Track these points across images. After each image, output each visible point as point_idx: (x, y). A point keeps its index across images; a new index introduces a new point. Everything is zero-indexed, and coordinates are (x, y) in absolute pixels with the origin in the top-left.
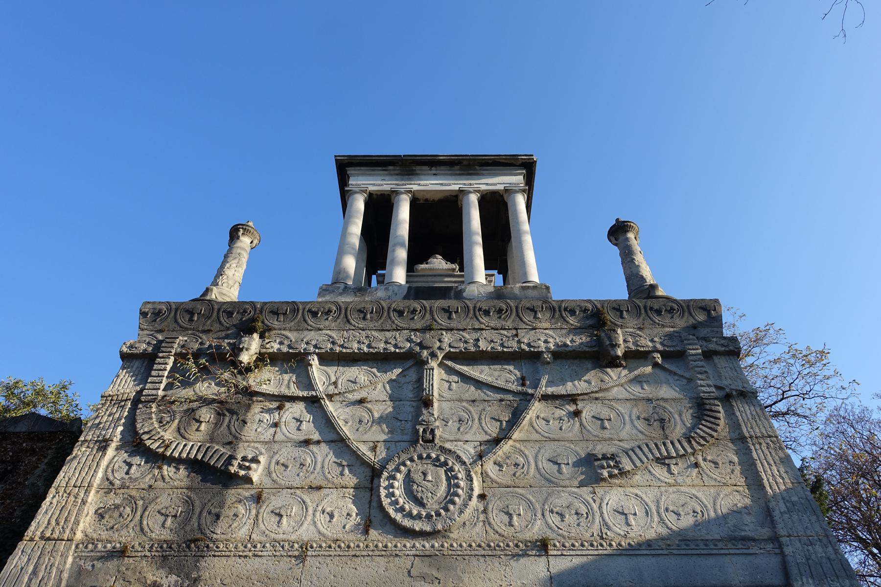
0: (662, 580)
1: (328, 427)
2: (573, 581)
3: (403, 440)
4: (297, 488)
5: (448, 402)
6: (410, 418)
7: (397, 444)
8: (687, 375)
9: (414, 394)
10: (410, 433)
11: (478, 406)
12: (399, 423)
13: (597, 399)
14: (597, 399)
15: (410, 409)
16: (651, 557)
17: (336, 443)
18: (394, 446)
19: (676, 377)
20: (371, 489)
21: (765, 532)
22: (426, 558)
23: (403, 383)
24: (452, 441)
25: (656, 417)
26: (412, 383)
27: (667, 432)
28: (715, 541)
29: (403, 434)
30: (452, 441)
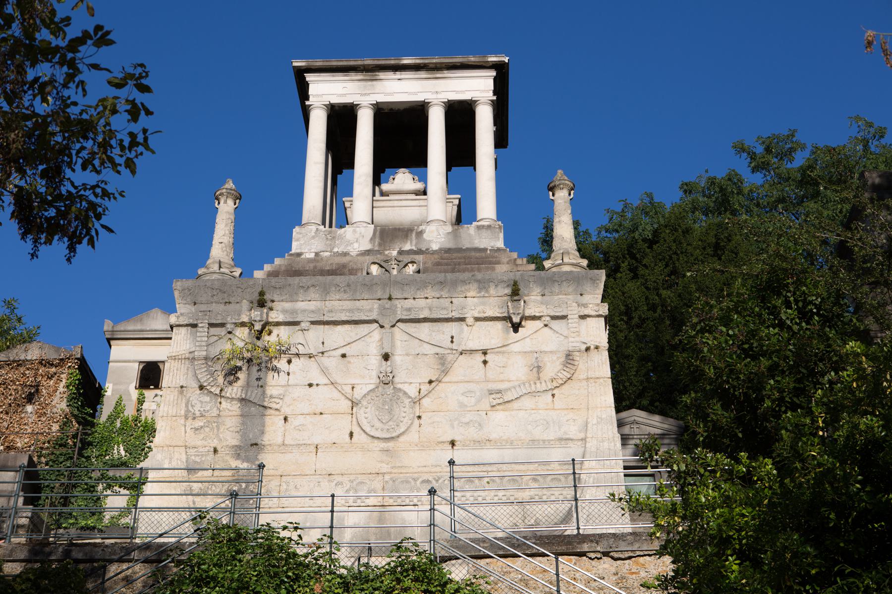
8: (565, 333)
12: (368, 371)
13: (500, 352)
14: (500, 352)
15: (375, 362)
19: (557, 335)
20: (352, 414)
21: (582, 435)
25: (536, 365)
27: (541, 375)
28: (549, 441)
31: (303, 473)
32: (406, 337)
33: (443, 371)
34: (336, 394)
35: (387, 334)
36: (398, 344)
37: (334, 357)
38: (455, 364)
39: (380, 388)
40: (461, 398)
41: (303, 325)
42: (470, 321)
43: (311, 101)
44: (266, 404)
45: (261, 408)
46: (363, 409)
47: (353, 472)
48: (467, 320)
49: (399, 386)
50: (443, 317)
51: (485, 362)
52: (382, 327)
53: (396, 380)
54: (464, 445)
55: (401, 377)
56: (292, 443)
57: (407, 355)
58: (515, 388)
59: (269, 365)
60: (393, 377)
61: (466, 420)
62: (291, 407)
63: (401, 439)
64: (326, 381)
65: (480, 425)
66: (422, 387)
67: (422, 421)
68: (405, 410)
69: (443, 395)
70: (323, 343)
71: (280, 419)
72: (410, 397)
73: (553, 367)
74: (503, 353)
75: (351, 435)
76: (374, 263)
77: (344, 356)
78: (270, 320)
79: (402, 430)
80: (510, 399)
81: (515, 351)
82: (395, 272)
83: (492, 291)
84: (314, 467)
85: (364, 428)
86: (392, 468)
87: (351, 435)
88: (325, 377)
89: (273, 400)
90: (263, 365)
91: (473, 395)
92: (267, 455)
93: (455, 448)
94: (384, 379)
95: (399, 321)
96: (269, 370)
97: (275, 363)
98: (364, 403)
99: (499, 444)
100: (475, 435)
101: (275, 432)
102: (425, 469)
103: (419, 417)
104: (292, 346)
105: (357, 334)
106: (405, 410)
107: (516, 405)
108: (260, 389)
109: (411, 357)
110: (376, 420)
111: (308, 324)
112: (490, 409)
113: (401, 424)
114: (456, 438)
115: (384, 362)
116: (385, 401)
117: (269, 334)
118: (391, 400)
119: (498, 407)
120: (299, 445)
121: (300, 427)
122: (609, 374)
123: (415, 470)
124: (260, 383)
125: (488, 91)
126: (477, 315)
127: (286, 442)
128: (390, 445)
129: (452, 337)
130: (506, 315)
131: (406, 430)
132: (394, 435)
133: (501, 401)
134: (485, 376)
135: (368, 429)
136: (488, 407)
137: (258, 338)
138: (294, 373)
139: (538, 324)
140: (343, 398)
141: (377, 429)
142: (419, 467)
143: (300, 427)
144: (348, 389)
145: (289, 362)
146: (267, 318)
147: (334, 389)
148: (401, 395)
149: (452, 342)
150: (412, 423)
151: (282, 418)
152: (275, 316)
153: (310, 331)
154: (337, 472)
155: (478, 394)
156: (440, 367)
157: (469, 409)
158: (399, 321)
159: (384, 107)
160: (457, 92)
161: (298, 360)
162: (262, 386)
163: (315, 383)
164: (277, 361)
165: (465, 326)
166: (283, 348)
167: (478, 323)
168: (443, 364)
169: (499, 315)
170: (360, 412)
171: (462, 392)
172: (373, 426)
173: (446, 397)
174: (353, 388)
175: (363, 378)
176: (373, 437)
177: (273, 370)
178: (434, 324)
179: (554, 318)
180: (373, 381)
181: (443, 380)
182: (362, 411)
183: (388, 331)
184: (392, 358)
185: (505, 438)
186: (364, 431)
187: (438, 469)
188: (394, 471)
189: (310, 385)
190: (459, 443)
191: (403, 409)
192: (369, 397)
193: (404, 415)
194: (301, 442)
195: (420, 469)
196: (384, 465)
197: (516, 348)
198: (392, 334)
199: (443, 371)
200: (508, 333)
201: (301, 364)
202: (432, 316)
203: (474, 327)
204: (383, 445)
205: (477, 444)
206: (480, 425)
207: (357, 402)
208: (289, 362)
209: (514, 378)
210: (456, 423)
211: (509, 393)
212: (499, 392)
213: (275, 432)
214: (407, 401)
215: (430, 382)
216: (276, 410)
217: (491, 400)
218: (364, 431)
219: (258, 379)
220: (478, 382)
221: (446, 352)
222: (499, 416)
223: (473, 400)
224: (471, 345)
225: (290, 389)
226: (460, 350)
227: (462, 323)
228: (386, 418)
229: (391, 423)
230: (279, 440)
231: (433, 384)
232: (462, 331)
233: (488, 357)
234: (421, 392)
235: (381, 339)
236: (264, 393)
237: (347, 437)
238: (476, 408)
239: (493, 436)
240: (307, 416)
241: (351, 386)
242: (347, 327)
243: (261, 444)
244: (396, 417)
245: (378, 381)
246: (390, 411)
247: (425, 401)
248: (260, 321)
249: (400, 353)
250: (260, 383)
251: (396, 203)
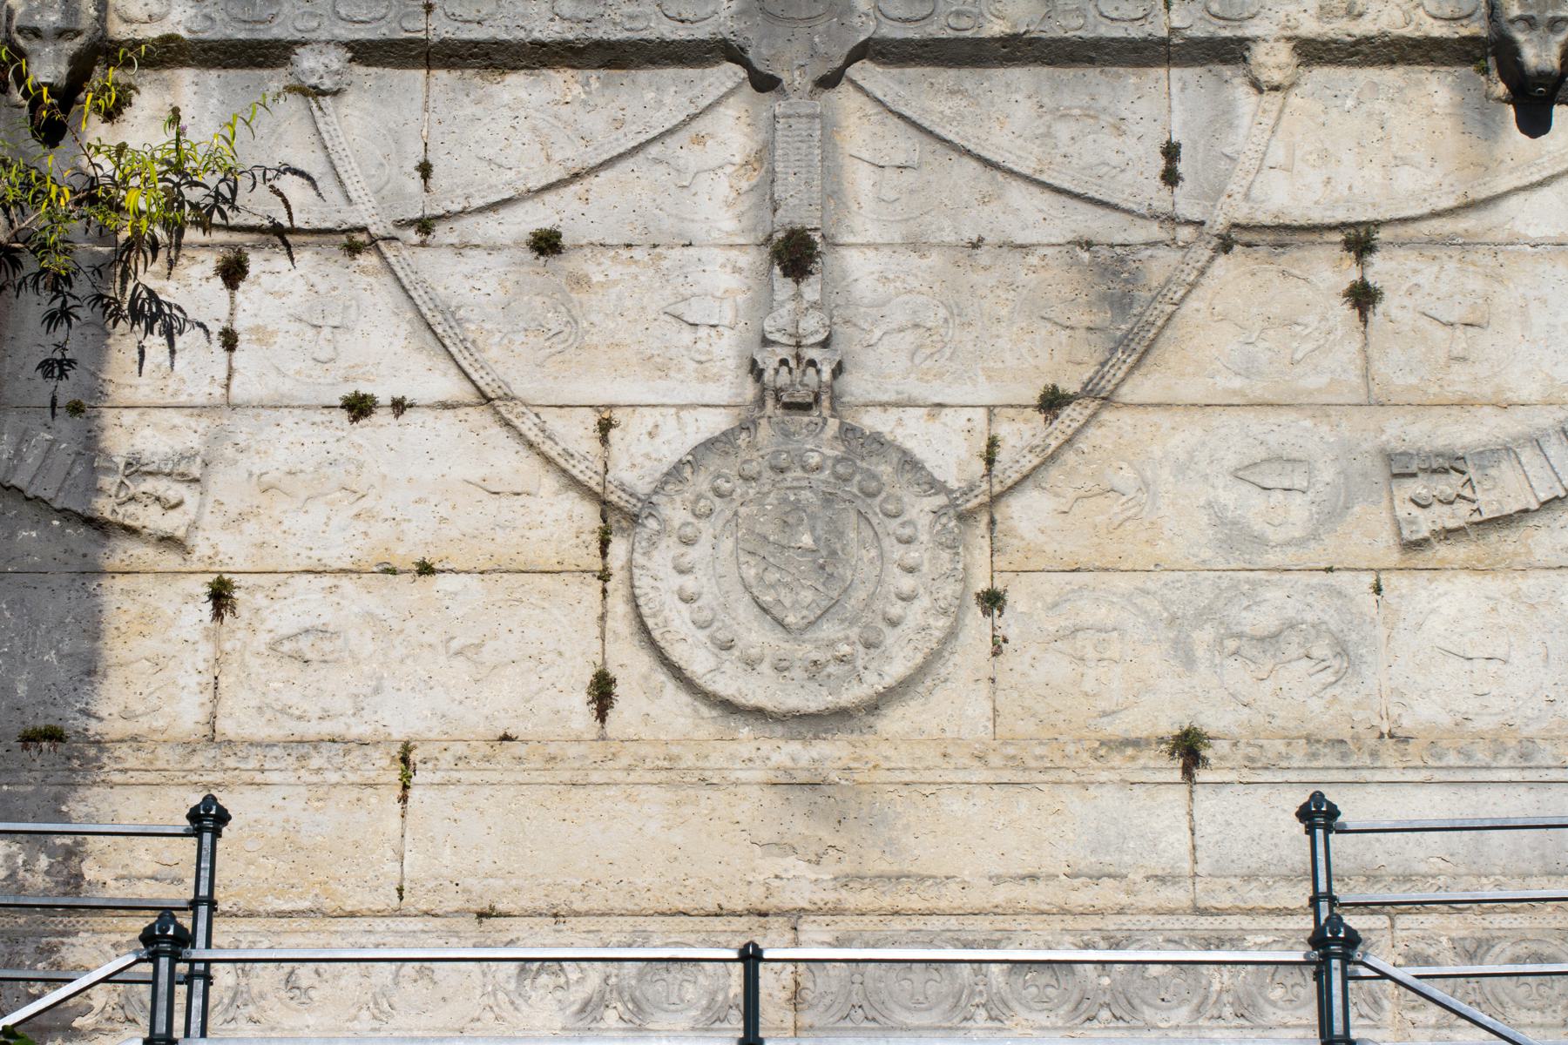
0: (1543, 856)
1: (420, 350)
2: (1264, 857)
3: (706, 400)
4: (342, 571)
5: (871, 253)
6: (728, 316)
7: (683, 414)
9: (739, 217)
10: (730, 377)
11: (985, 269)
12: (687, 336)
13: (1447, 242)
14: (1447, 242)
16: (1522, 789)
17: (461, 412)
18: (671, 422)
22: (797, 791)
23: (693, 169)
24: (884, 405)
26: (729, 169)
29: (704, 378)
30: (884, 405)
31: (329, 905)
32: (904, 145)
33: (1124, 343)
34: (509, 462)
35: (801, 126)
36: (861, 181)
37: (493, 249)
38: (1192, 303)
39: (764, 432)
40: (1230, 496)
41: (310, 64)
42: (1273, 60)
44: (104, 507)
45: (76, 533)
47: (617, 902)
48: (1259, 54)
49: (872, 421)
50: (1117, 32)
51: (1363, 297)
52: (764, 83)
53: (856, 385)
54: (1251, 763)
56: (262, 731)
57: (915, 245)
58: (1537, 443)
59: (114, 291)
60: (838, 370)
61: (1262, 620)
62: (250, 527)
63: (894, 721)
65: (1342, 649)
66: (1004, 430)
67: (1009, 624)
68: (913, 555)
69: (1125, 478)
70: (425, 170)
71: (190, 598)
72: (935, 486)
74: (1466, 244)
75: (602, 691)
77: (546, 244)
78: (119, 30)
79: (897, 669)
80: (1512, 507)
81: (1534, 233)
84: (392, 868)
85: (677, 653)
86: (845, 881)
87: (602, 691)
88: (443, 364)
89: (149, 485)
90: (82, 287)
91: (1299, 481)
92: (117, 795)
93: (1202, 775)
94: (784, 378)
95: (863, 51)
96: (117, 316)
97: (149, 276)
98: (675, 512)
99: (1452, 759)
100: (1316, 705)
101: (158, 667)
102: (1034, 895)
103: (992, 601)
104: (244, 182)
105: (619, 123)
106: (913, 555)
108: (66, 425)
109: (935, 259)
110: (744, 609)
111: (336, 59)
112: (1394, 558)
113: (890, 636)
114: (1209, 721)
115: (784, 287)
116: (797, 506)
117: (111, 115)
118: (828, 499)
119: (1443, 551)
120: (301, 747)
121: (304, 644)
123: (975, 900)
124: (66, 391)
126: (1310, 27)
127: (226, 727)
128: (830, 752)
129: (1171, 152)
130: (1477, 28)
131: (922, 671)
132: (851, 695)
133: (1460, 515)
134: (1366, 375)
135: (698, 661)
136: (1385, 550)
137: (52, 133)
138: (262, 335)
140: (550, 482)
141: (751, 664)
142: (997, 880)
143: (304, 644)
144: (576, 434)
145: (233, 272)
146: (102, 19)
147: (497, 433)
148: (885, 470)
149: (1171, 177)
150: (952, 634)
151: (200, 587)
153: (350, 98)
154: (525, 902)
155: (1327, 474)
156: (1102, 317)
157: (1274, 558)
158: (863, 51)
161: (281, 261)
162: (76, 409)
163: (384, 396)
164: (160, 265)
165: (1241, 93)
166: (193, 195)
167: (1320, 74)
168: (1121, 303)
169: (1438, 30)
171: (1232, 461)
172: (727, 646)
173: (1145, 486)
174: (605, 427)
175: (663, 370)
176: (729, 707)
177: (136, 314)
178: (1067, 74)
180: (720, 392)
181: (1127, 393)
182: (662, 558)
183: (805, 107)
184: (828, 261)
185: (1484, 723)
186: (677, 672)
187: (1108, 895)
188: (851, 899)
189: (359, 407)
190: (1222, 747)
191: (898, 552)
192: (702, 482)
193: (907, 583)
194: (312, 729)
195: (1001, 895)
196: (793, 865)
198: (829, 129)
199: (1124, 343)
200: (1489, 130)
201: (300, 288)
202: (1053, 31)
203: (1294, 100)
205: (1329, 758)
206: (1342, 649)
207: (632, 506)
208: (233, 272)
209: (1529, 390)
210: (1203, 637)
211: (1506, 472)
212: (1449, 464)
213: (158, 667)
214: (921, 508)
215: (1052, 402)
216: (168, 541)
217: (1404, 510)
218: (677, 672)
219: (56, 367)
220: (1322, 409)
221: (1141, 232)
223: (1299, 512)
225: (242, 427)
226: (1219, 222)
227: (1227, 71)
228: (800, 601)
229: (829, 630)
230: (188, 715)
231: (1071, 415)
232: (1224, 118)
233: (1380, 269)
234: (1003, 456)
235: (763, 157)
236: (90, 446)
237: (579, 704)
238: (1316, 555)
239: (1422, 713)
240: (345, 582)
241: (592, 419)
242: (561, 82)
243: (83, 735)
244: (861, 594)
245: (750, 390)
246: (826, 562)
248: (61, 34)
249: (872, 233)
250: (66, 391)
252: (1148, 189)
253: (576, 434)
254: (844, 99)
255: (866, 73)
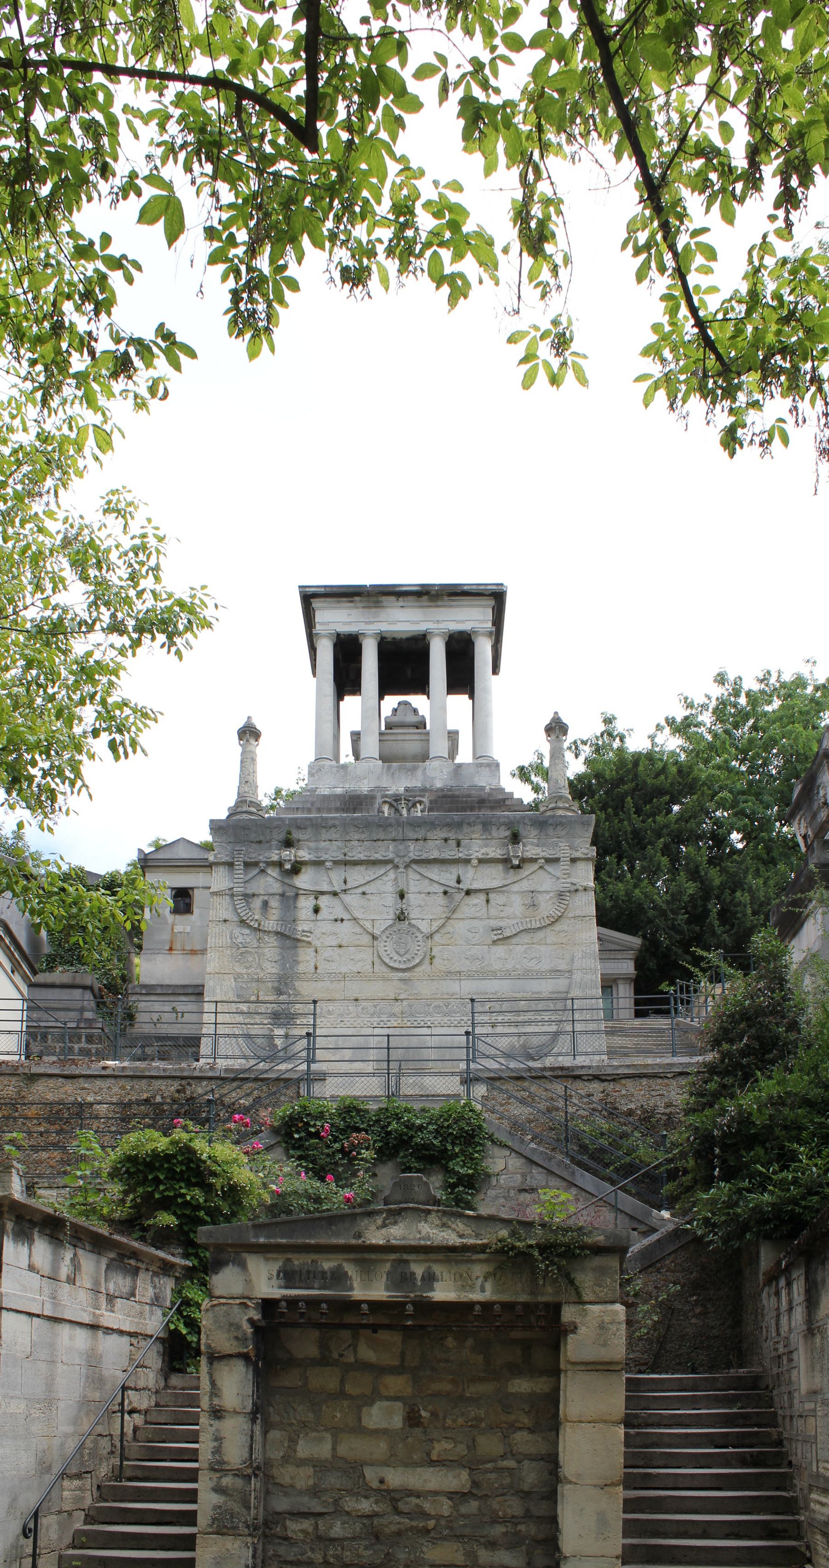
32: (418, 877)
34: (358, 930)
36: (411, 882)
43: (318, 628)
46: (383, 944)
49: (413, 922)
52: (396, 867)
55: (414, 913)
63: (417, 970)
64: (349, 917)
73: (547, 907)
74: (503, 892)
76: (385, 802)
77: (364, 893)
82: (404, 812)
83: (495, 833)
107: (514, 941)
122: (594, 913)
125: (486, 621)
126: (480, 856)
135: (387, 961)
139: (535, 866)
152: (304, 854)
159: (387, 635)
160: (457, 622)
170: (380, 945)
176: (392, 968)
179: (548, 861)
192: (387, 932)
197: (516, 888)
204: (400, 975)
214: (420, 936)
222: (500, 951)
224: (475, 886)
235: (396, 879)
247: (437, 937)
251: (400, 737)
252: (453, 883)
253: (368, 925)
254: (410, 871)
255: (414, 866)
